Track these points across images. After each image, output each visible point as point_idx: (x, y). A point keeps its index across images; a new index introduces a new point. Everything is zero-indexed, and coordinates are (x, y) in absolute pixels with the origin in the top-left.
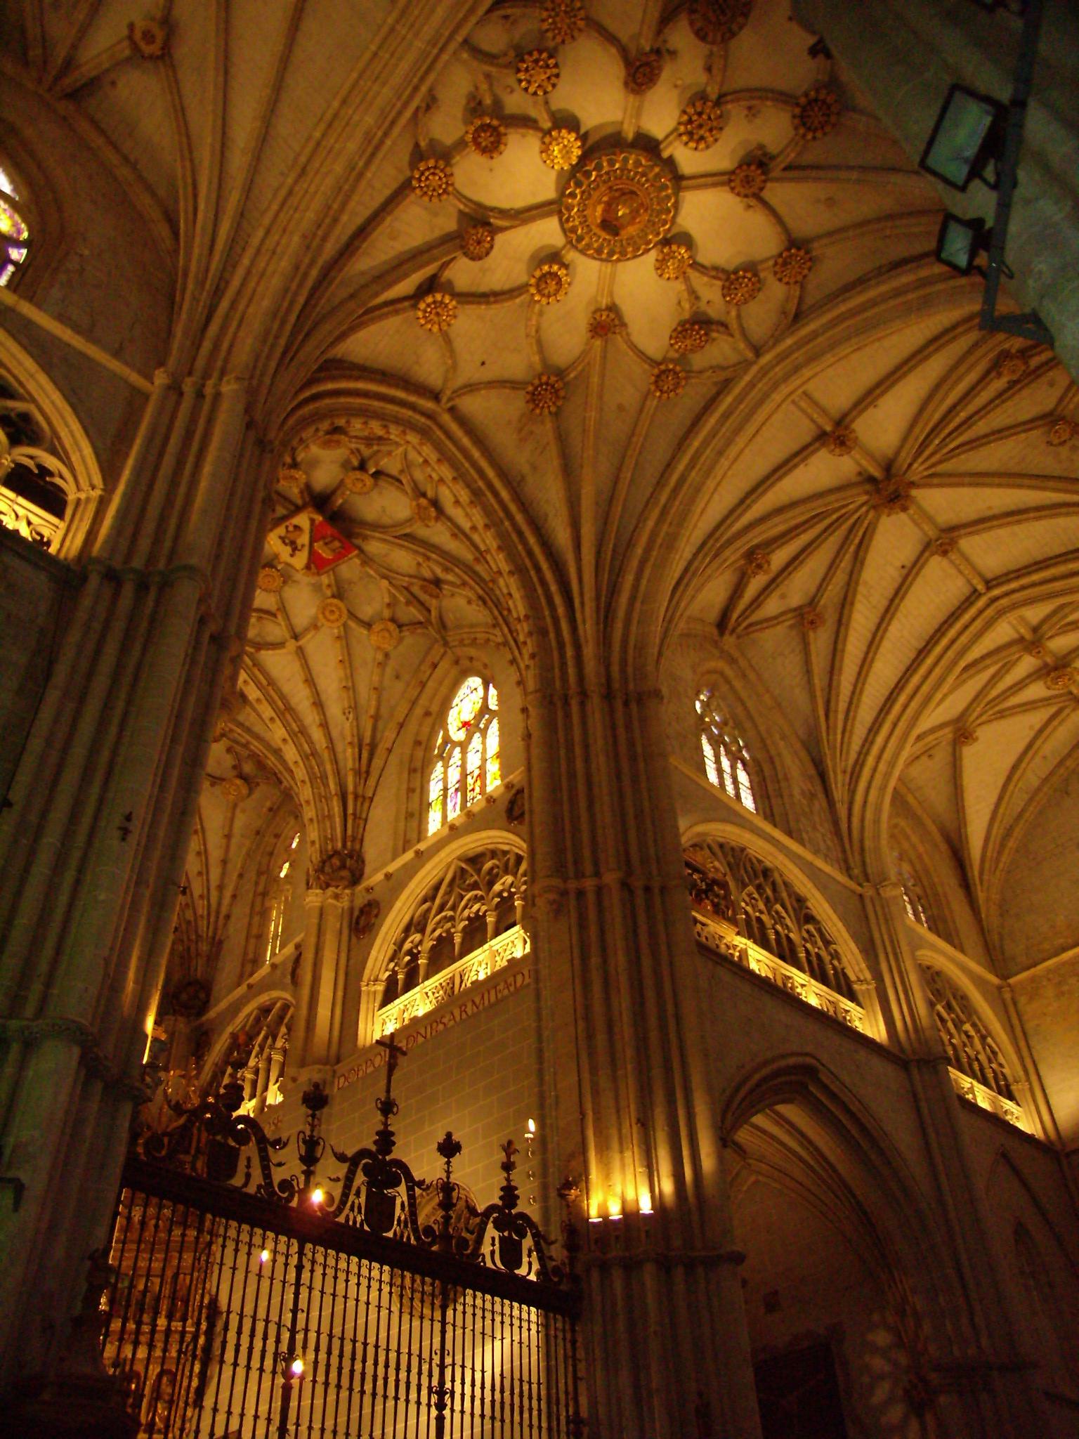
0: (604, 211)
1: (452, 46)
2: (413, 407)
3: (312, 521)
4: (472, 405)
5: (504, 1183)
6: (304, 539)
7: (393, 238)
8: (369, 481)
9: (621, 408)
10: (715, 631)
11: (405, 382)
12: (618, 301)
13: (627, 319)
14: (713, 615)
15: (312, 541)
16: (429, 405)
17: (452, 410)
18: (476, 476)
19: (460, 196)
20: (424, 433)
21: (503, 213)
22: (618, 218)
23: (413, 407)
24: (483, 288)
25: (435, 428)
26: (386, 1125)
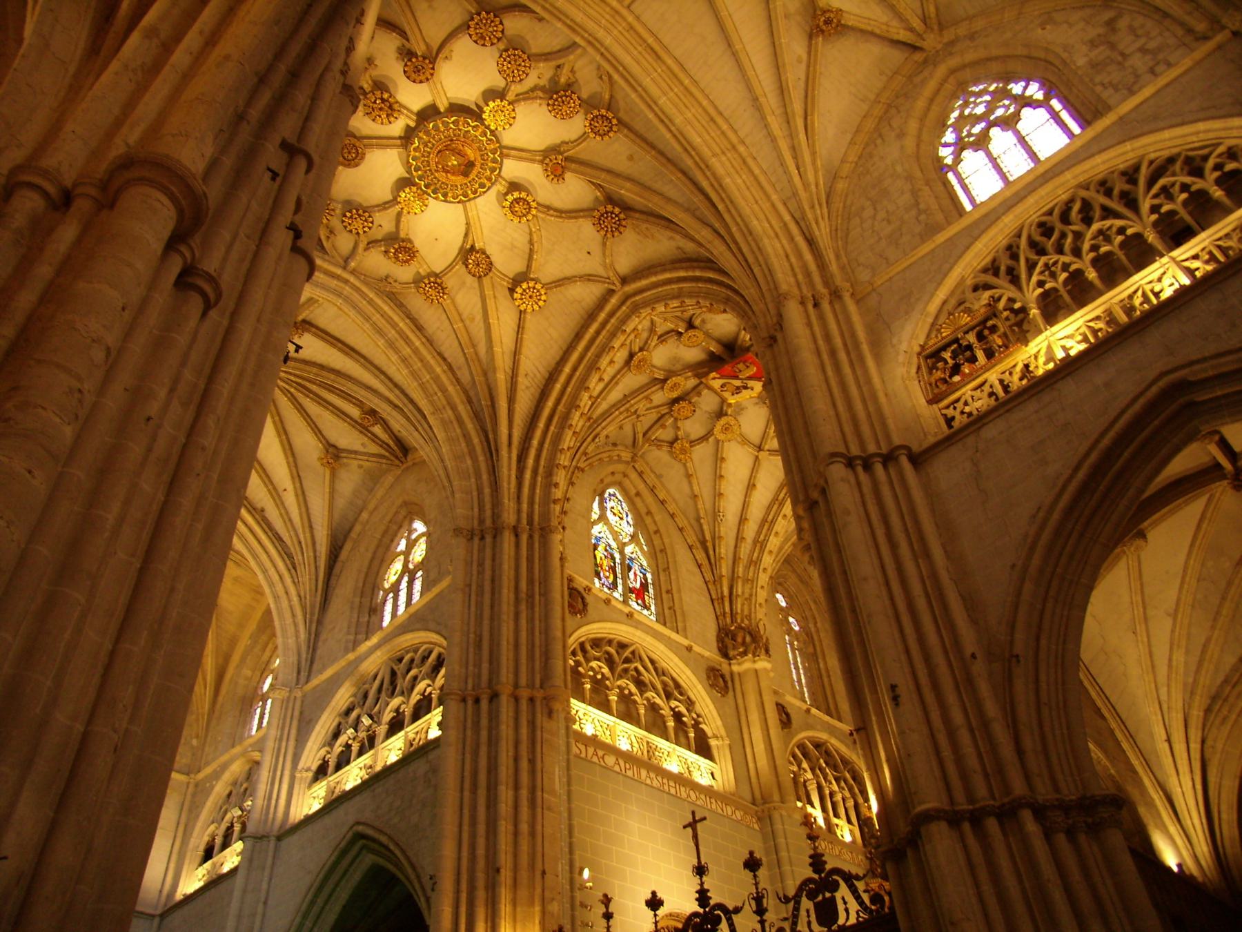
0: (453, 174)
1: (346, 275)
2: (612, 314)
3: (714, 378)
4: (624, 264)
5: (812, 852)
6: (737, 383)
7: (473, 319)
8: (691, 333)
9: (631, 158)
10: (918, 57)
11: (591, 316)
12: (542, 148)
13: (558, 141)
14: (897, 56)
15: (737, 377)
16: (614, 301)
17: (624, 280)
18: (668, 287)
19: (450, 267)
20: (635, 309)
21: (466, 235)
22: (459, 165)
23: (612, 314)
24: (527, 251)
25: (633, 299)
26: (702, 884)
